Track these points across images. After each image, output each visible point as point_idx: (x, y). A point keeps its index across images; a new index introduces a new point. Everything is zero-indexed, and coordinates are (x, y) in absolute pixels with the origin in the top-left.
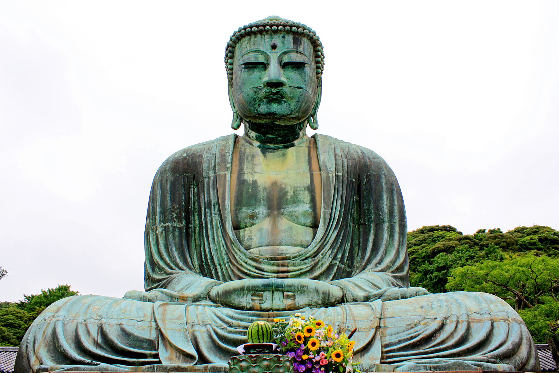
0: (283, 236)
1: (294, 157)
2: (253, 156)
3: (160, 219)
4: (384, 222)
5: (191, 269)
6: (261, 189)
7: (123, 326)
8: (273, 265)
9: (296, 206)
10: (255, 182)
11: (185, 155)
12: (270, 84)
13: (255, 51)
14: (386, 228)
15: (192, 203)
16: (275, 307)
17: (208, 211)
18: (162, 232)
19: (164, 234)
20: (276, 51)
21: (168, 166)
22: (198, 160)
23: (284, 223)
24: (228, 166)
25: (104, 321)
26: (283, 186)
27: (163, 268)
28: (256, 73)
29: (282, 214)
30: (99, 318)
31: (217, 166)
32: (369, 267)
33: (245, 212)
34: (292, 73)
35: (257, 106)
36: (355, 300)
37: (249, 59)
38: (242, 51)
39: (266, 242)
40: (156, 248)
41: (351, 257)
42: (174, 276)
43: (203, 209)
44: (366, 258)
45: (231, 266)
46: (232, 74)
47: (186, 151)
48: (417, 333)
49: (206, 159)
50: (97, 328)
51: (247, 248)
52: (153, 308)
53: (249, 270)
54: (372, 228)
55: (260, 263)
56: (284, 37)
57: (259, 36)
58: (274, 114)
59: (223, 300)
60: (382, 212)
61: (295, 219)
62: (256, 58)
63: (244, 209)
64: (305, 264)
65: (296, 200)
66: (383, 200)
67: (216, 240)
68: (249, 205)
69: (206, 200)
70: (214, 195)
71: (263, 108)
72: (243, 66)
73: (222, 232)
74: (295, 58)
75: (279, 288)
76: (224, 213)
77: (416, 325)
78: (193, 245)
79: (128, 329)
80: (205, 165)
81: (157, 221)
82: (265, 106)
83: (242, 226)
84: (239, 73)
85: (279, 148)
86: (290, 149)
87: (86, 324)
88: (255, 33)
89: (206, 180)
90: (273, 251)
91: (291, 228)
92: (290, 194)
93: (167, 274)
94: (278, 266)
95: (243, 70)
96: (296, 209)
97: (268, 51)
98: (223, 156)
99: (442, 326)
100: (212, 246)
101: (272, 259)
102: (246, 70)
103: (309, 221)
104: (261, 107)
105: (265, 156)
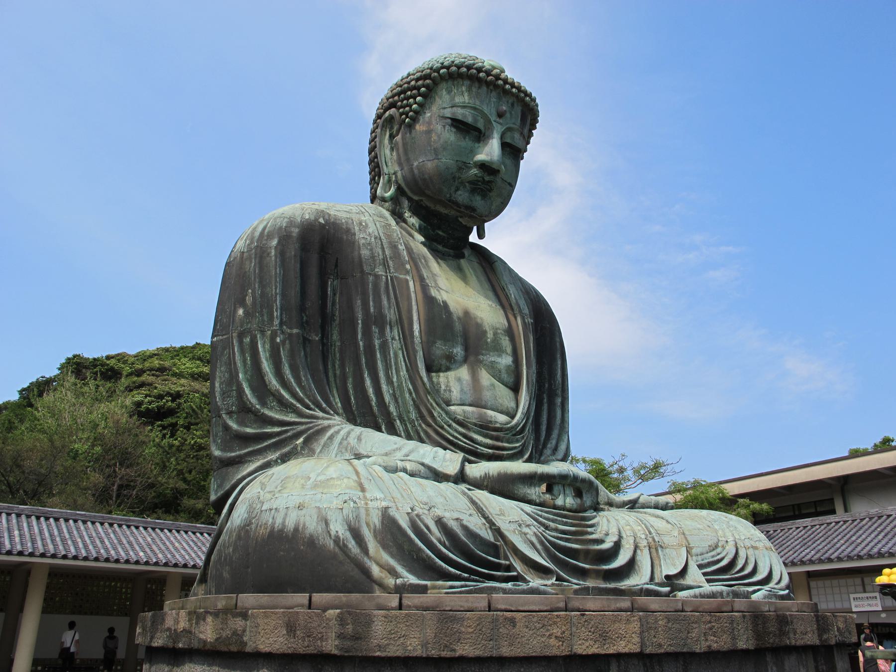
0: (487, 395)
1: (474, 278)
3: (281, 320)
4: (556, 395)
5: (338, 414)
6: (455, 318)
7: (465, 523)
8: (486, 436)
9: (500, 356)
10: (445, 303)
11: (322, 221)
12: (483, 166)
13: (475, 109)
14: (559, 404)
15: (329, 304)
16: (568, 505)
17: (375, 329)
18: (283, 342)
19: (287, 346)
20: (501, 121)
21: (295, 231)
22: (345, 237)
23: (485, 378)
24: (408, 267)
25: (439, 512)
26: (479, 321)
27: (292, 404)
28: (467, 143)
29: (481, 362)
30: (427, 507)
31: (391, 263)
32: (548, 452)
33: (440, 348)
34: (508, 162)
35: (453, 189)
37: (464, 115)
38: (453, 99)
39: (469, 398)
40: (271, 366)
42: (326, 423)
43: (360, 322)
44: (542, 439)
45: (423, 426)
46: (414, 120)
47: (322, 213)
48: (719, 557)
49: (363, 241)
50: (433, 522)
51: (448, 403)
52: (464, 494)
53: (456, 438)
54: (545, 400)
55: (468, 429)
56: (513, 105)
57: (484, 88)
58: (473, 209)
60: (555, 381)
61: (496, 374)
62: (476, 120)
63: (439, 344)
64: (517, 441)
65: (498, 349)
66: (557, 365)
67: (395, 380)
68: (445, 340)
69: (372, 310)
70: (390, 307)
72: (449, 121)
73: (407, 371)
76: (413, 342)
77: (716, 547)
78: (331, 374)
79: (472, 527)
80: (365, 253)
81: (276, 322)
82: (467, 194)
83: (434, 368)
84: (439, 127)
85: (449, 255)
86: (462, 261)
87: (418, 516)
89: (371, 278)
90: (481, 417)
91: (493, 385)
92: (490, 335)
93: (300, 414)
94: (492, 438)
95: (447, 127)
96: (499, 360)
97: (493, 118)
98: (394, 247)
100: (384, 387)
101: (481, 426)
102: (454, 130)
103: (511, 380)
104: (459, 192)
105: (438, 263)
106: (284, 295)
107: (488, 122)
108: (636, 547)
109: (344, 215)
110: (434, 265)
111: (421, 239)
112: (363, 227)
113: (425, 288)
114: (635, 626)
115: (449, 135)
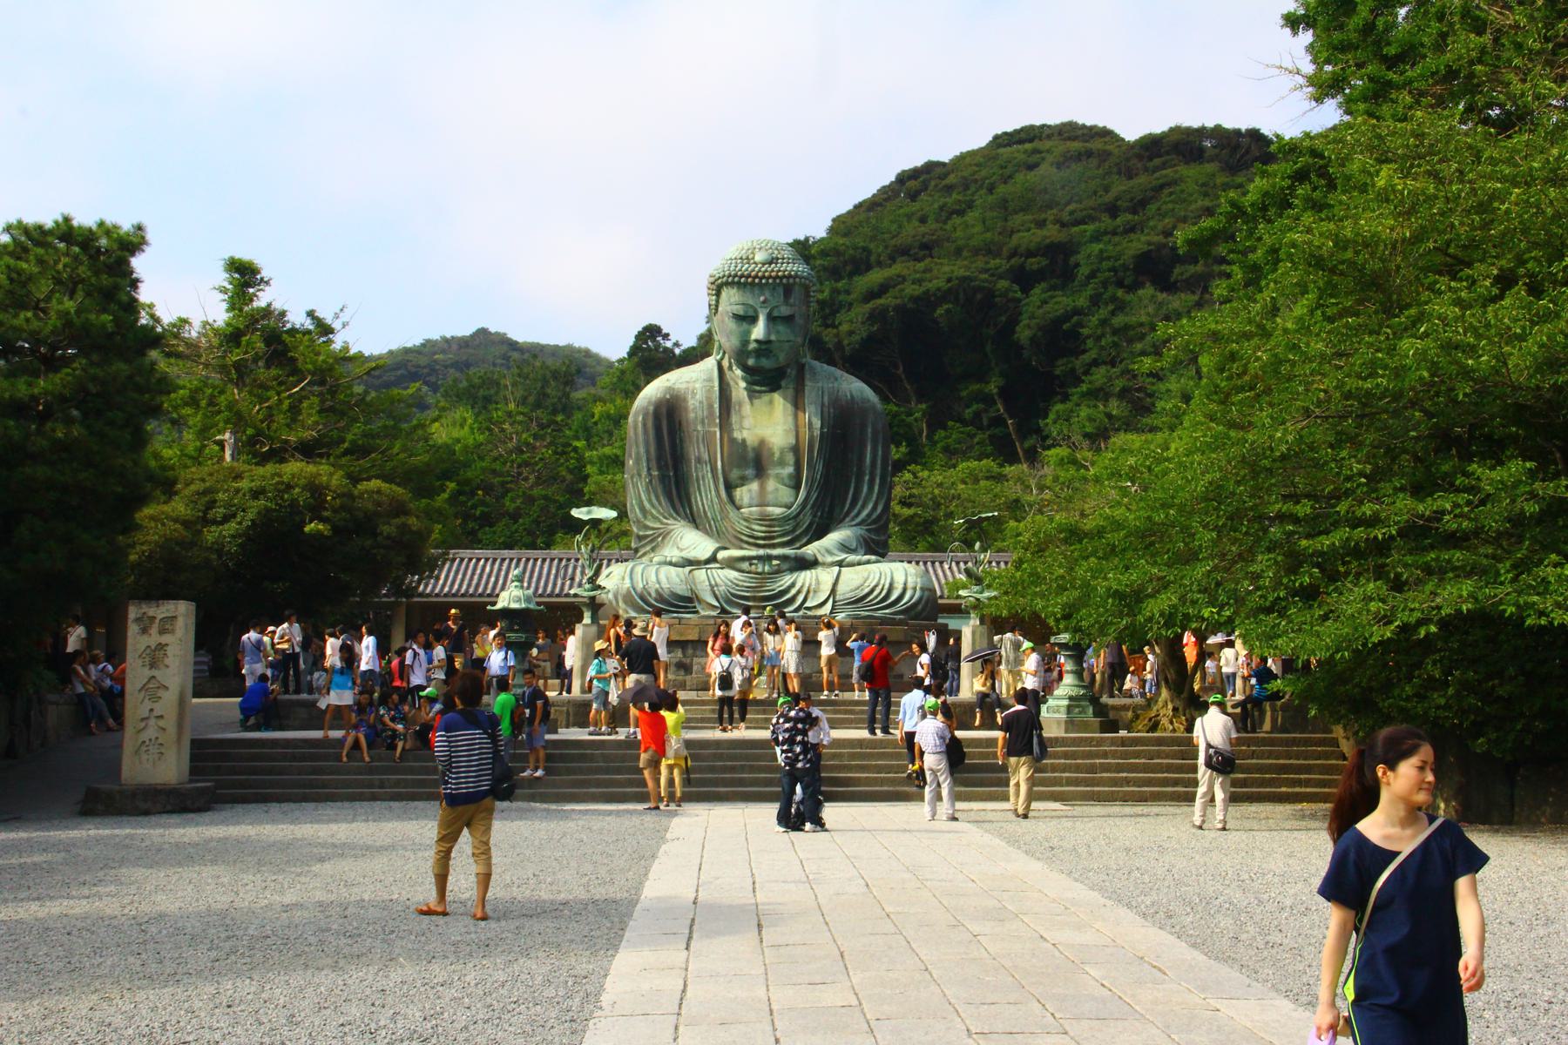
0: (770, 497)
2: (740, 405)
10: (744, 441)
23: (771, 485)
28: (745, 326)
34: (781, 328)
36: (824, 564)
41: (831, 512)
47: (669, 389)
51: (738, 508)
59: (731, 564)
65: (782, 463)
68: (739, 466)
71: (751, 362)
74: (785, 311)
75: (769, 558)
80: (692, 415)
88: (745, 284)
92: (777, 455)
98: (711, 406)
99: (872, 591)
106: (648, 452)
107: (756, 311)
108: (799, 592)
109: (683, 386)
110: (747, 408)
111: (743, 384)
112: (694, 394)
113: (731, 431)
114: (697, 630)
115: (731, 325)
